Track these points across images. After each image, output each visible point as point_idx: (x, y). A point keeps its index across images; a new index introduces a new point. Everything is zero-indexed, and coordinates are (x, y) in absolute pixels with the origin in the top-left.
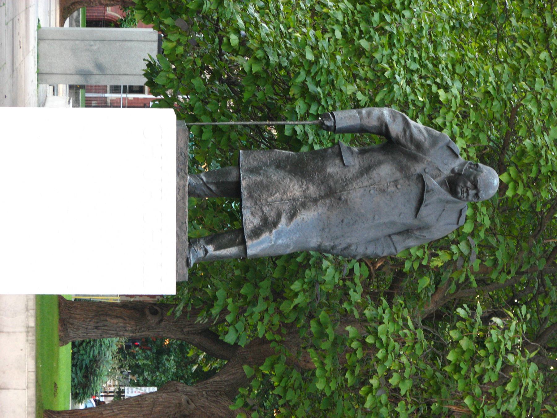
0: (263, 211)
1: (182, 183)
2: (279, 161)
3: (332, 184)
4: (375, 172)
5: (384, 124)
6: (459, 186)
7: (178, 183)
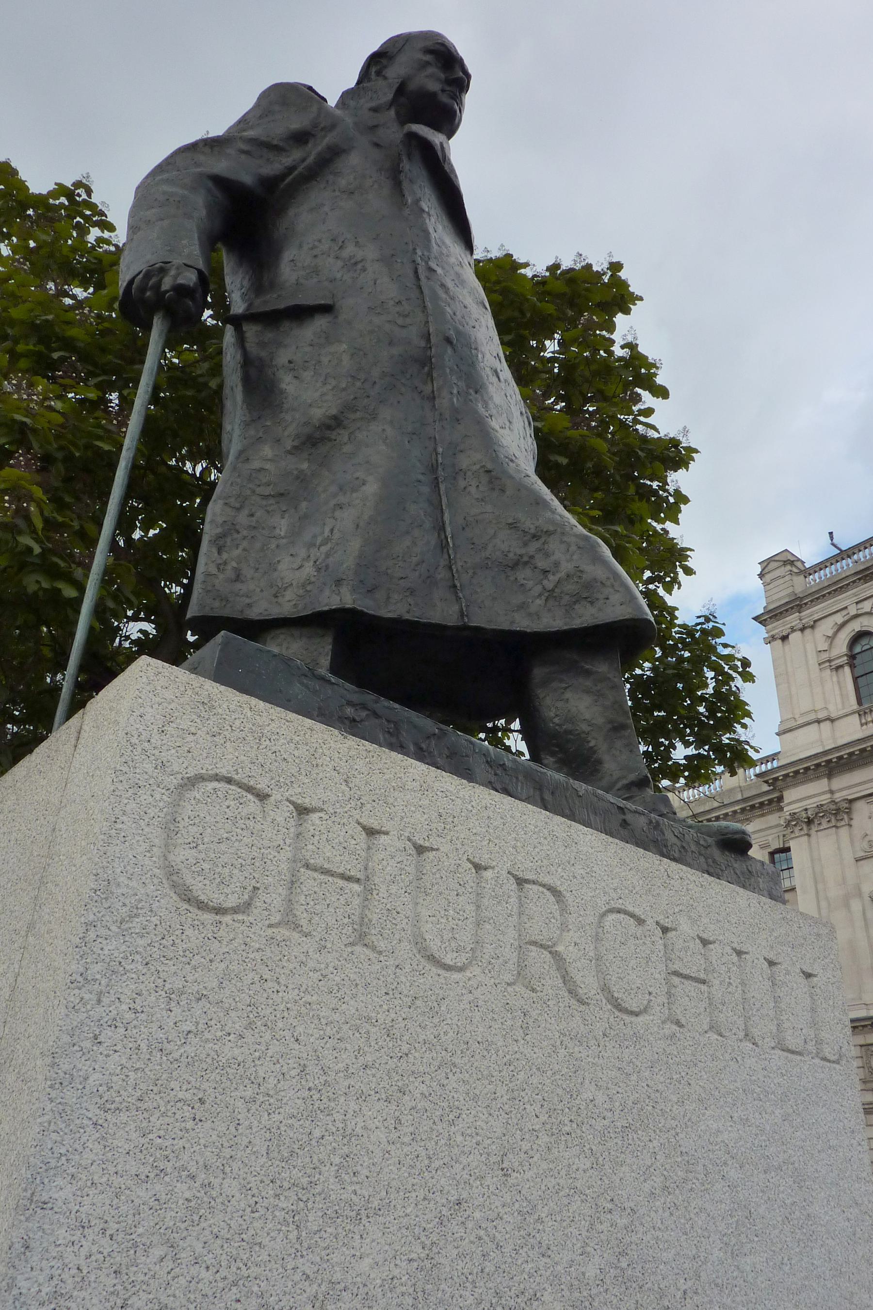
2: (265, 497)
5: (210, 184)
6: (434, 95)
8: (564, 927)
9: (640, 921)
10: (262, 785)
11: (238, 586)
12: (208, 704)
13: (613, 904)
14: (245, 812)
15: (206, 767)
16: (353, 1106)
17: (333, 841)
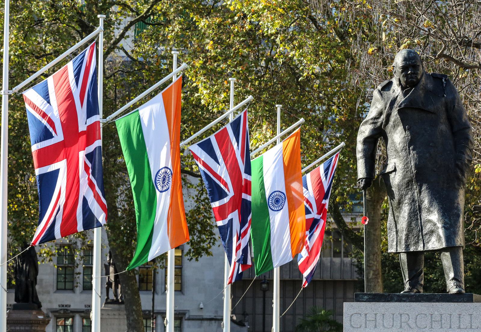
0: (426, 234)
3: (407, 179)
4: (398, 147)
7: (396, 301)
8: (409, 319)
9: (426, 315)
10: (360, 313)
12: (352, 306)
15: (353, 313)
17: (370, 317)
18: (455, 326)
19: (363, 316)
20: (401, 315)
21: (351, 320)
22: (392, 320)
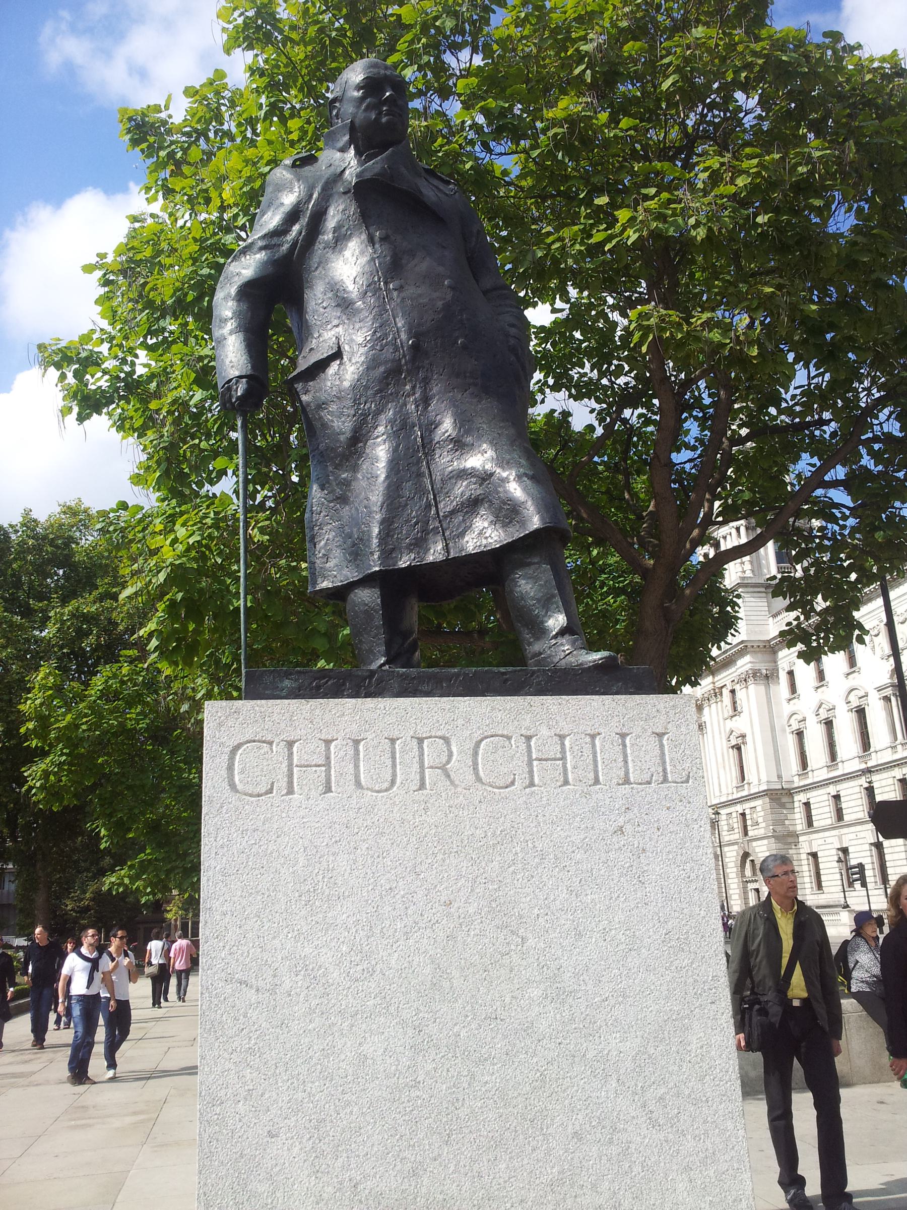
0: (453, 512)
1: (395, 684)
3: (382, 369)
9: (509, 738)
10: (269, 738)
11: (328, 565)
13: (486, 734)
14: (262, 751)
16: (331, 858)
18: (610, 773)
19: (279, 749)
20: (421, 741)
21: (230, 768)
22: (389, 762)
